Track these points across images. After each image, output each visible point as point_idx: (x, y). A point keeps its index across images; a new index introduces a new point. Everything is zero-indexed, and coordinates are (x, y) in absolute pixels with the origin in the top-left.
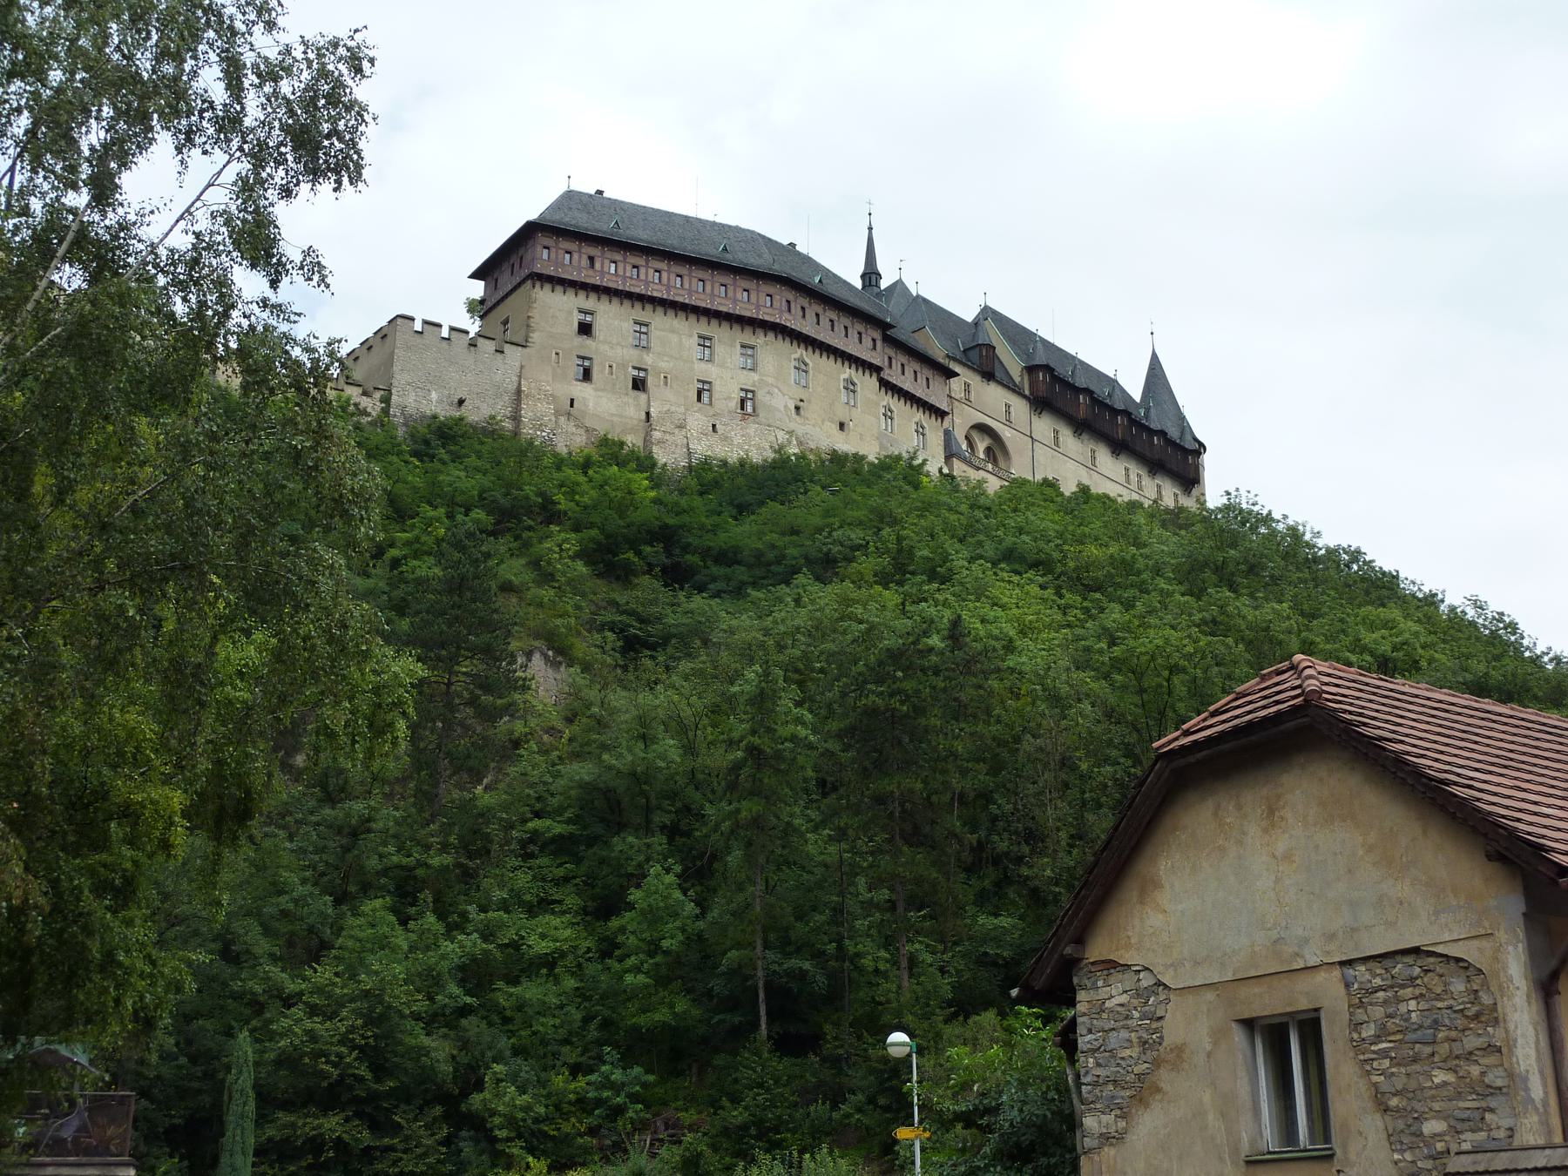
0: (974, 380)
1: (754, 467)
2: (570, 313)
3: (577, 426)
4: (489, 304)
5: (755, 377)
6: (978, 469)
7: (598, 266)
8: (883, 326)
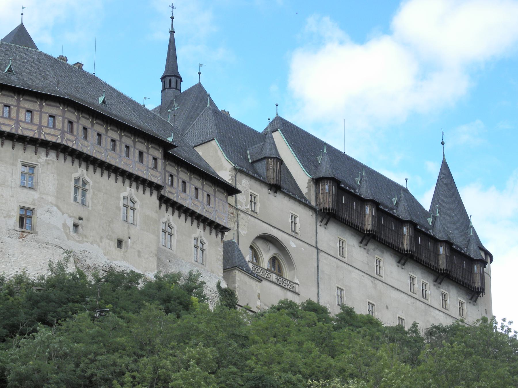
1: (30, 285)
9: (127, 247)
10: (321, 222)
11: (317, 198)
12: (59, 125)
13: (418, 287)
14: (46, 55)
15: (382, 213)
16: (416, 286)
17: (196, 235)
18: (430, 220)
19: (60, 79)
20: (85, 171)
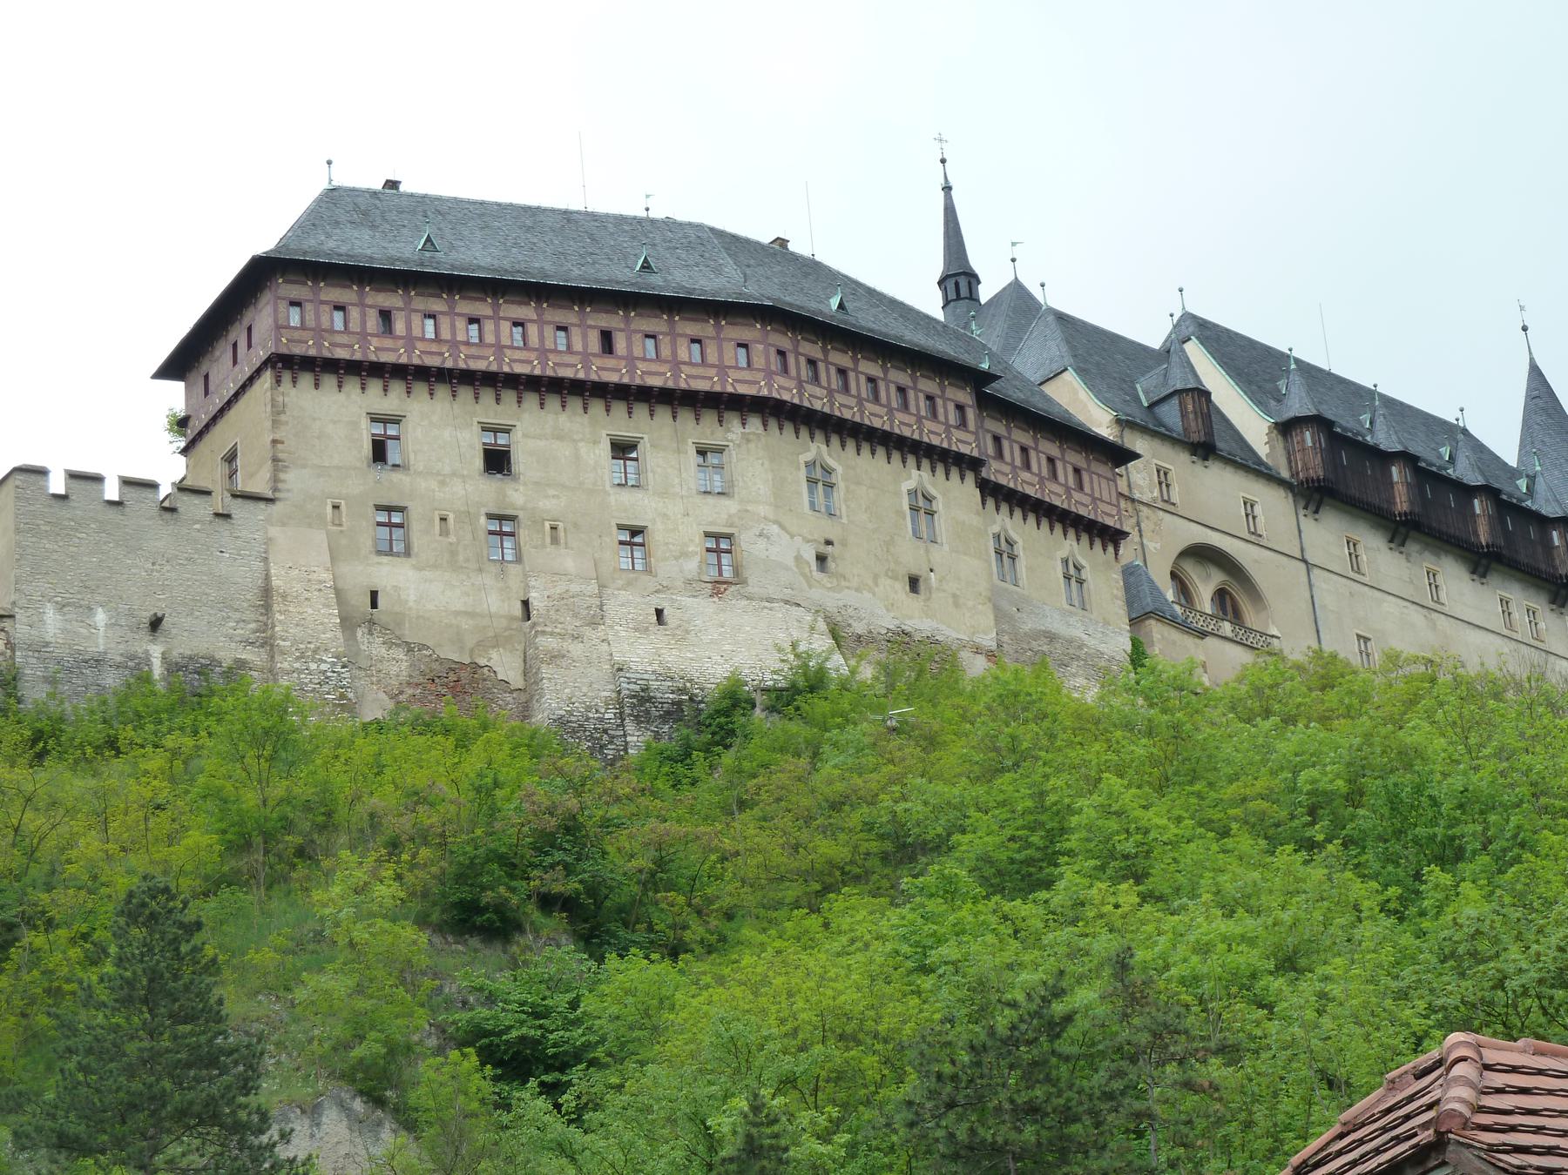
0: (1179, 463)
2: (354, 425)
3: (389, 644)
4: (196, 425)
5: (730, 506)
6: (1203, 634)
7: (399, 327)
8: (977, 380)
9: (930, 589)
10: (1306, 508)
11: (1290, 462)
12: (759, 362)
13: (1519, 616)
14: (712, 230)
15: (1427, 477)
16: (1516, 615)
17: (1063, 553)
18: (1522, 484)
19: (748, 271)
20: (824, 447)
